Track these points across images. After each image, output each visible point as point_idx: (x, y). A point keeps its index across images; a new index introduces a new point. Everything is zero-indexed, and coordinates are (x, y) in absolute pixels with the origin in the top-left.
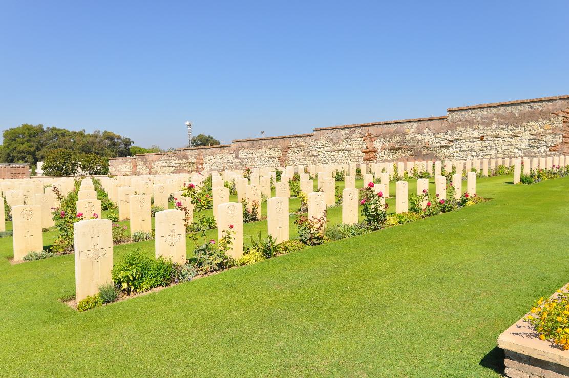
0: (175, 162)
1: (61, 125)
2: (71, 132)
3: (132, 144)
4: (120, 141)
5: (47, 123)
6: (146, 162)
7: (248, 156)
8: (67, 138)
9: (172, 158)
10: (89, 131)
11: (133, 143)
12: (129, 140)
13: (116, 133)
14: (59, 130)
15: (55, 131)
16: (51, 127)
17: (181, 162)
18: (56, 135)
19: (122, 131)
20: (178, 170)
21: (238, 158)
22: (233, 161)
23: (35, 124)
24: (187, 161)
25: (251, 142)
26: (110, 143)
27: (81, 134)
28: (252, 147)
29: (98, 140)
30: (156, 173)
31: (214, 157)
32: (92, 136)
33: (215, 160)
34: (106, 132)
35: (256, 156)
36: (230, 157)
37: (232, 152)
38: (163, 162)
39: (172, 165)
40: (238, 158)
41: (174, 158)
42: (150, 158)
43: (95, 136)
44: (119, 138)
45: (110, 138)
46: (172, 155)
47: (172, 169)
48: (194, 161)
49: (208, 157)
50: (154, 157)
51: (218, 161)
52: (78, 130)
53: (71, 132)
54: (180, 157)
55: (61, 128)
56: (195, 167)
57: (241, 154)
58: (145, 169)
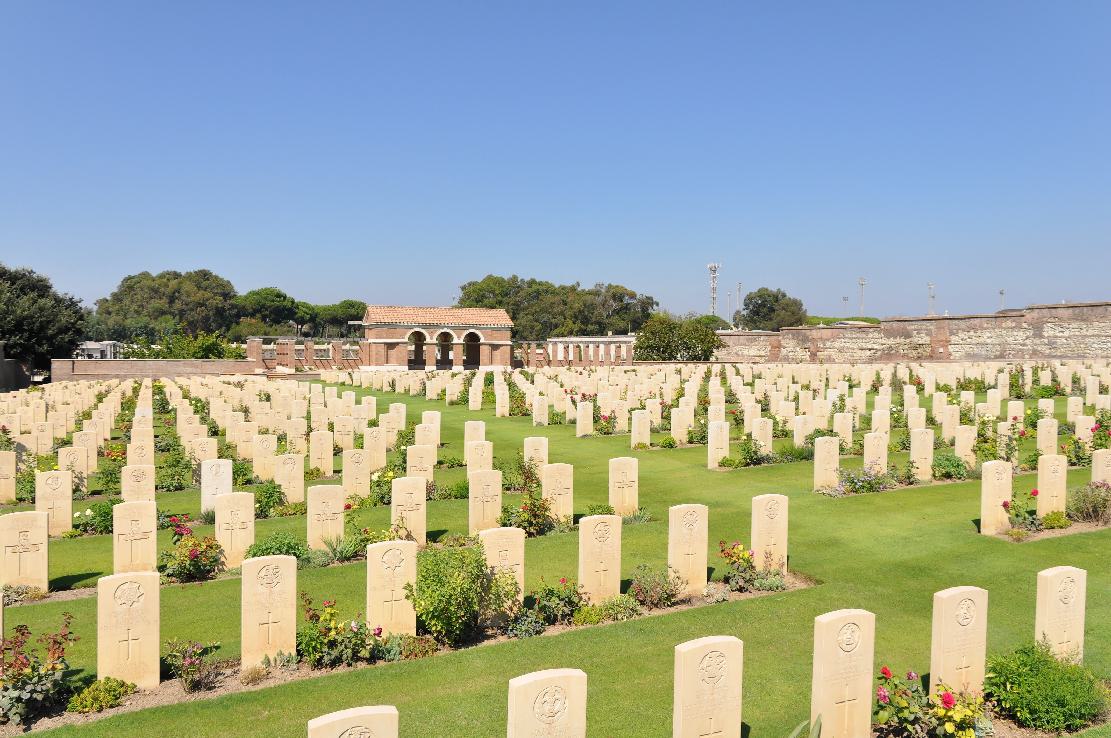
0: (877, 341)
1: (540, 277)
2: (557, 286)
3: (655, 307)
4: (635, 302)
5: (525, 275)
6: (804, 341)
7: (1067, 334)
8: (549, 298)
9: (871, 335)
10: (587, 285)
11: (657, 304)
12: (650, 298)
13: (630, 288)
14: (540, 284)
15: (535, 287)
16: (527, 279)
17: (891, 341)
18: (538, 293)
19: (640, 288)
20: (888, 355)
21: (1042, 337)
22: (1028, 342)
23: (506, 276)
24: (908, 341)
25: (1077, 310)
26: (615, 305)
27: (573, 289)
28: (1076, 319)
29: (599, 300)
30: (830, 360)
31: (979, 333)
32: (590, 293)
33: (981, 340)
34: (610, 285)
35: (1090, 332)
36: (1020, 335)
37: (1025, 325)
38: (850, 343)
39: (870, 347)
40: (1042, 337)
41: (876, 335)
42: (815, 334)
43: (596, 293)
44: (633, 296)
45: (618, 295)
46: (871, 330)
47: (868, 353)
48: (926, 339)
49: (962, 335)
50: (827, 333)
51: (989, 341)
52: (569, 283)
53: (557, 286)
54: (889, 334)
55: (544, 280)
56: (929, 350)
57: (1049, 331)
58: (801, 353)
